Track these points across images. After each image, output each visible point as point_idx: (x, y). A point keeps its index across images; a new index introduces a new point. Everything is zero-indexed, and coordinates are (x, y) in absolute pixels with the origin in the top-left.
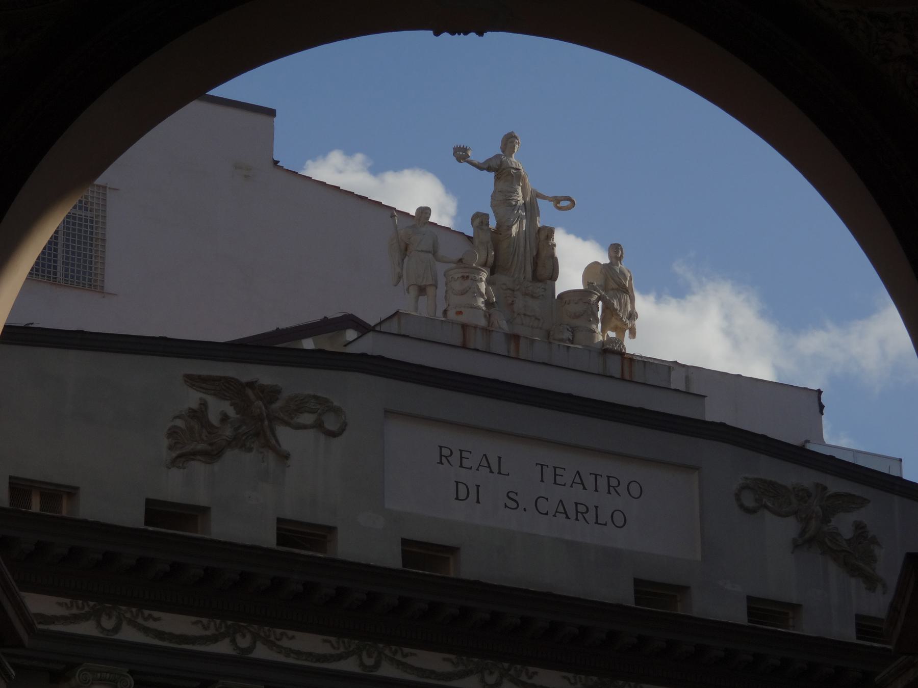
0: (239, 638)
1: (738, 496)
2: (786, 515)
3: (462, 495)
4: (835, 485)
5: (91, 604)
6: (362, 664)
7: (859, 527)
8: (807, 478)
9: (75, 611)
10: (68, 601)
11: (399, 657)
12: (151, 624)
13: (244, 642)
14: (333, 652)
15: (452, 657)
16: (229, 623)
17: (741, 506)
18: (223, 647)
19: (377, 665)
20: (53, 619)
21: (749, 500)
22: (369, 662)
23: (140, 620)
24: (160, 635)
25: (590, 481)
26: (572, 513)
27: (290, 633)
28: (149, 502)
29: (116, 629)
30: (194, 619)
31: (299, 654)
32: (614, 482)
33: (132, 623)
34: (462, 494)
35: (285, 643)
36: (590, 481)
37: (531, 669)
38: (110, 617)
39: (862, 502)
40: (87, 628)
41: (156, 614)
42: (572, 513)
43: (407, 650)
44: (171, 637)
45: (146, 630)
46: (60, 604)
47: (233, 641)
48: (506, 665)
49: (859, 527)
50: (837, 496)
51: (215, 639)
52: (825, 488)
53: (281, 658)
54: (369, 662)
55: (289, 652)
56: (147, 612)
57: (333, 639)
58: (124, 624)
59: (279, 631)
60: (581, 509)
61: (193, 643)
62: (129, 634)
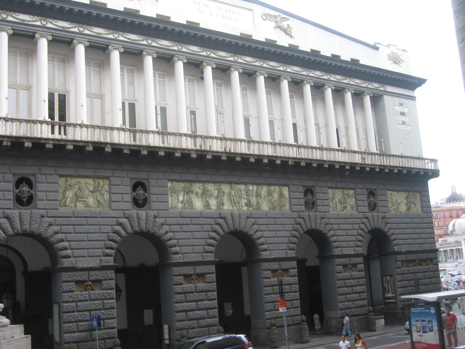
0: (148, 40)
1: (262, 17)
2: (273, 21)
3: (200, 12)
4: (283, 16)
5: (112, 31)
6: (178, 48)
7: (288, 26)
8: (277, 13)
9: (108, 32)
10: (106, 30)
11: (187, 47)
12: (126, 36)
13: (150, 42)
14: (171, 45)
15: (200, 48)
16: (146, 37)
17: (263, 18)
18: (145, 42)
19: (182, 48)
20: (102, 34)
21: (264, 17)
22: (180, 48)
23: (124, 35)
24: (129, 39)
25: (229, 11)
26: (225, 18)
27: (161, 40)
28: (124, 8)
29: (118, 37)
30: (137, 36)
31: (163, 45)
32: (234, 12)
33: (122, 36)
34: (200, 12)
35: (159, 42)
36: (229, 11)
37: (218, 51)
38: (116, 34)
39: (289, 19)
40: (111, 36)
41: (128, 34)
42: (225, 18)
43: (189, 46)
44: (132, 40)
45: (126, 38)
46: (104, 31)
47: (147, 41)
48: (212, 50)
49: (288, 25)
50: (283, 18)
51: (142, 41)
52: (280, 16)
53: (159, 46)
54: (180, 48)
55: (160, 45)
56: (125, 34)
57: (171, 42)
58: (120, 36)
59: (158, 40)
60: (227, 17)
61: (137, 41)
62: (121, 38)
